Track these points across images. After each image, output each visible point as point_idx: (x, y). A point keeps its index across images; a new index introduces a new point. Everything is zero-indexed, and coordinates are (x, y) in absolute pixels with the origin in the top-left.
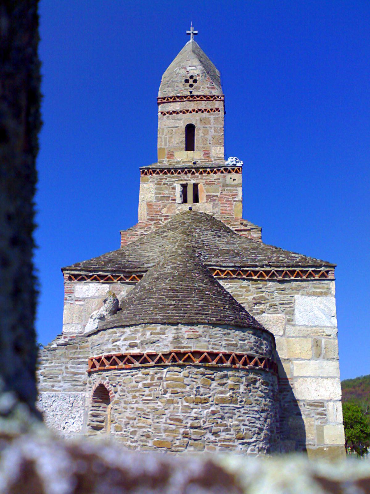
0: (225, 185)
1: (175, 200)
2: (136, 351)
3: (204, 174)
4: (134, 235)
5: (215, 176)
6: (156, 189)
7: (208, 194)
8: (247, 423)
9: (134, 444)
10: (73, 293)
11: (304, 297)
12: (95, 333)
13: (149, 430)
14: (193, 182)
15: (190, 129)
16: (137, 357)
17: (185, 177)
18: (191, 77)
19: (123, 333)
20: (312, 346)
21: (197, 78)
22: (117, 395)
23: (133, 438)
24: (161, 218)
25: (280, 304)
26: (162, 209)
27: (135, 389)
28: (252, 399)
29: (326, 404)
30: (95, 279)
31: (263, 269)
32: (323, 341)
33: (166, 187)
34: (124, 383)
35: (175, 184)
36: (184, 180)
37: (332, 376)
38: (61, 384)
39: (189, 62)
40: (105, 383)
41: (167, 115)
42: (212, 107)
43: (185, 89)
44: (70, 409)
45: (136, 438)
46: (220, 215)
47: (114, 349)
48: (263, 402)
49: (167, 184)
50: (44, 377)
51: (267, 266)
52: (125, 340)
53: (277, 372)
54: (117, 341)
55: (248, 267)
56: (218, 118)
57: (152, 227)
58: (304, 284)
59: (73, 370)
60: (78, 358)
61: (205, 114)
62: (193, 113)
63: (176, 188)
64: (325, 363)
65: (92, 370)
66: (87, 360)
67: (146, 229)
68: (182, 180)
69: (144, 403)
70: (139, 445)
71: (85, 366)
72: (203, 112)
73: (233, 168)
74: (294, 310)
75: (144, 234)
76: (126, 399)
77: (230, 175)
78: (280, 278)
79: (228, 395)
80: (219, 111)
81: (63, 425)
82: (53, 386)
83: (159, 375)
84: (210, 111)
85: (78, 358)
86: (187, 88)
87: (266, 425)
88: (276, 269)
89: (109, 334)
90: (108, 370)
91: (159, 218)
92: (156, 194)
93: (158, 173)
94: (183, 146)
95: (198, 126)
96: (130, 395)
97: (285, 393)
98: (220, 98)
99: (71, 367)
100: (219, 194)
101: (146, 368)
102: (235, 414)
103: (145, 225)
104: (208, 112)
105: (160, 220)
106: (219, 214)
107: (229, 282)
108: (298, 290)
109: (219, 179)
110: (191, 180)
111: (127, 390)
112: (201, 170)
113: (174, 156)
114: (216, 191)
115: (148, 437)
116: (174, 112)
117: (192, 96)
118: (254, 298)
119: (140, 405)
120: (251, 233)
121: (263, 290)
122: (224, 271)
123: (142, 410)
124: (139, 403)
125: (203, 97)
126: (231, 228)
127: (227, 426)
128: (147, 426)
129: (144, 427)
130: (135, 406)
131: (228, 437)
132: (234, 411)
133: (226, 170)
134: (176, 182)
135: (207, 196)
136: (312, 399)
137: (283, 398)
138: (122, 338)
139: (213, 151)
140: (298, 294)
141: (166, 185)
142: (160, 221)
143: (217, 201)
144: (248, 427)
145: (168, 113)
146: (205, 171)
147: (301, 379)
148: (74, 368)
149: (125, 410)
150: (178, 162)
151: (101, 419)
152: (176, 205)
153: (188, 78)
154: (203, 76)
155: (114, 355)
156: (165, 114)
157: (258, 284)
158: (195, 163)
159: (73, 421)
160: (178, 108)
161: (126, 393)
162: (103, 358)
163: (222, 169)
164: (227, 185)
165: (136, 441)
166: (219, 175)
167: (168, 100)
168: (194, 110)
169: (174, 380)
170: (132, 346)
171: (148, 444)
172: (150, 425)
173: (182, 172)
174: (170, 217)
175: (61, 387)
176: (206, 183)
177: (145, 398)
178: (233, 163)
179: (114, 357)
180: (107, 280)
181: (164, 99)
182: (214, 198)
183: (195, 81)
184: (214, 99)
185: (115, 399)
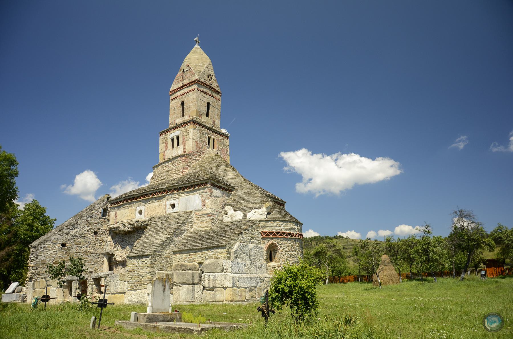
2: (289, 232)
14: (212, 137)
15: (209, 104)
16: (290, 234)
18: (210, 75)
22: (281, 249)
27: (289, 246)
30: (218, 187)
61: (215, 100)
77: (225, 140)
110: (213, 136)
116: (203, 91)
117: (211, 87)
119: (291, 252)
181: (199, 81)
183: (211, 78)
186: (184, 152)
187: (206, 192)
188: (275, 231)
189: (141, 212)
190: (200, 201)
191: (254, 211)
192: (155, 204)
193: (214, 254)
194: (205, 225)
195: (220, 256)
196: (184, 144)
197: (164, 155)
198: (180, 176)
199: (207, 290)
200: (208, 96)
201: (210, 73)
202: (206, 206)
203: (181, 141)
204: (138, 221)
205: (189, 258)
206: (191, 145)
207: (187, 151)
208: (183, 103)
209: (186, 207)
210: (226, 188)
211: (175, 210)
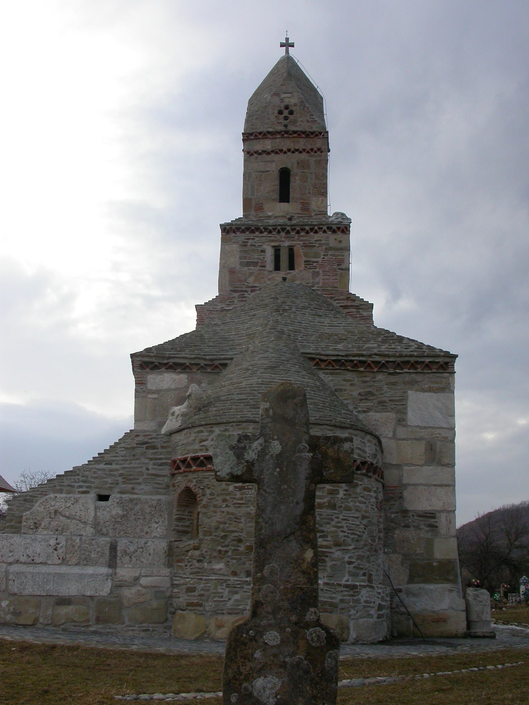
1: (264, 266)
3: (302, 234)
4: (213, 311)
5: (316, 237)
6: (241, 251)
7: (306, 259)
8: (345, 529)
9: (224, 549)
10: (145, 384)
11: (418, 393)
12: (179, 431)
13: (241, 534)
14: (287, 244)
17: (278, 237)
18: (287, 107)
19: (212, 432)
20: (426, 450)
23: (223, 543)
24: (247, 289)
25: (390, 400)
26: (249, 277)
28: (351, 504)
29: (438, 515)
31: (371, 359)
32: (439, 444)
33: (254, 250)
34: (213, 486)
35: (264, 246)
36: (277, 241)
37: (445, 483)
38: (143, 486)
39: (284, 88)
40: (191, 485)
41: (255, 155)
42: (313, 147)
43: (278, 123)
44: (153, 513)
46: (321, 287)
47: (201, 450)
48: (364, 508)
49: (255, 245)
50: (123, 478)
51: (376, 355)
53: (382, 478)
54: (204, 441)
55: (354, 356)
56: (319, 160)
57: (236, 301)
58: (419, 378)
59: (154, 472)
60: (160, 459)
61: (304, 156)
62: (289, 153)
63: (266, 252)
64: (439, 468)
65: (176, 472)
66: (170, 461)
67: (228, 303)
68: (273, 241)
69: (235, 507)
70: (230, 549)
71: (167, 468)
72: (301, 152)
73: (339, 226)
74: (406, 409)
75: (226, 310)
76: (216, 503)
77: (334, 236)
78: (391, 371)
79: (326, 500)
80: (322, 152)
81: (146, 529)
82: (133, 489)
84: (310, 151)
85: (160, 459)
86: (281, 121)
87: (366, 533)
88: (387, 359)
89: (195, 433)
90: (195, 471)
91: (244, 289)
92: (241, 258)
93: (243, 232)
94: (277, 196)
95: (295, 170)
96: (220, 499)
97: (392, 502)
98: (323, 135)
99: (153, 469)
100: (320, 260)
102: (332, 520)
103: (226, 297)
104: (308, 152)
105: (245, 291)
106: (320, 285)
107: (331, 374)
108: (412, 384)
109: (321, 240)
111: (216, 493)
112: (298, 228)
113: (263, 209)
114: (316, 255)
115: (240, 541)
116: (264, 152)
117: (287, 132)
118: (360, 394)
119: (231, 509)
120: (360, 310)
121: (371, 383)
122: (325, 361)
123: (233, 514)
124: (229, 507)
125: (301, 134)
126: (335, 303)
127: (323, 532)
128: (238, 530)
129: (236, 531)
130: (226, 509)
131: (324, 543)
132: (332, 517)
133: (329, 228)
134: (266, 243)
135: (305, 262)
136: (423, 509)
137: (390, 509)
138: (210, 438)
139: (313, 203)
140: (412, 389)
141: (253, 247)
142: (245, 293)
143: (318, 268)
144: (346, 534)
145: (256, 152)
146: (303, 230)
147: (412, 487)
148: (155, 469)
149: (215, 514)
150: (269, 217)
151: (188, 523)
152: (266, 273)
153: (282, 108)
154: (301, 105)
155: (202, 456)
156: (252, 155)
157: (365, 377)
158: (290, 219)
160: (269, 147)
161: (215, 496)
162: (189, 459)
163: (325, 228)
164: (331, 249)
165: (228, 546)
166: (321, 235)
167: (256, 135)
168: (289, 150)
171: (239, 548)
172: (242, 529)
173: (275, 229)
174: (258, 288)
175: (142, 489)
176: (305, 246)
177: (235, 501)
178: (338, 220)
179: (202, 458)
180: (184, 369)
181: (251, 134)
182: (315, 264)
183: (291, 113)
184: (315, 136)
185: (204, 502)
200: (282, 155)
201: (282, 105)
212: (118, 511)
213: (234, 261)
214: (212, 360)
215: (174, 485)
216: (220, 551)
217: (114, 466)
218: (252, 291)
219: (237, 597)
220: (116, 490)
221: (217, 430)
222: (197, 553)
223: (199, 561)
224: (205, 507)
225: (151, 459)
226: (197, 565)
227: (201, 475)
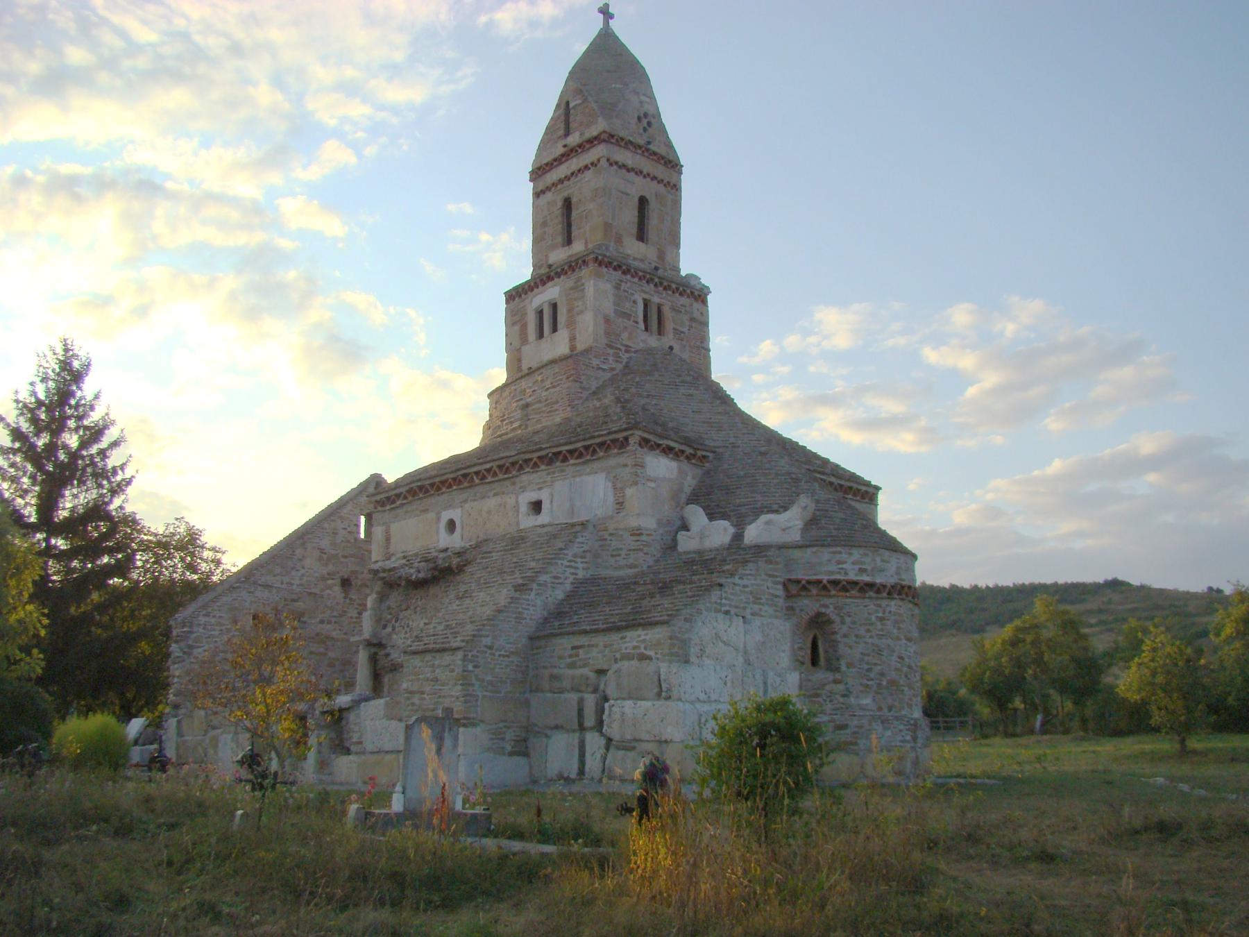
0: (692, 319)
2: (866, 578)
14: (656, 300)
15: (643, 202)
16: (871, 585)
18: (646, 115)
19: (850, 554)
21: (653, 121)
22: (845, 629)
38: (766, 608)
45: (872, 675)
52: (853, 563)
57: (611, 358)
61: (661, 188)
83: (888, 609)
92: (616, 304)
93: (615, 269)
94: (634, 231)
95: (653, 204)
100: (685, 330)
101: (877, 598)
112: (665, 284)
116: (623, 166)
117: (647, 150)
138: (850, 561)
145: (616, 163)
156: (611, 165)
159: (782, 655)
169: (900, 615)
170: (862, 571)
176: (673, 309)
181: (612, 136)
183: (649, 124)
186: (573, 348)
187: (625, 465)
188: (825, 578)
189: (451, 525)
190: (610, 492)
191: (764, 518)
192: (492, 502)
193: (635, 647)
194: (622, 562)
195: (651, 653)
196: (571, 324)
197: (519, 360)
198: (558, 420)
199: (618, 748)
202: (627, 504)
203: (562, 318)
204: (446, 550)
205: (570, 656)
206: (591, 329)
207: (580, 347)
208: (568, 204)
209: (572, 512)
210: (689, 451)
211: (544, 518)
212: (759, 637)
213: (608, 306)
214: (696, 449)
215: (791, 609)
216: (867, 686)
217: (745, 582)
218: (626, 351)
219: (888, 733)
220: (748, 611)
221: (856, 554)
222: (840, 687)
223: (844, 696)
224: (845, 636)
225: (770, 576)
226: (841, 700)
227: (841, 601)
